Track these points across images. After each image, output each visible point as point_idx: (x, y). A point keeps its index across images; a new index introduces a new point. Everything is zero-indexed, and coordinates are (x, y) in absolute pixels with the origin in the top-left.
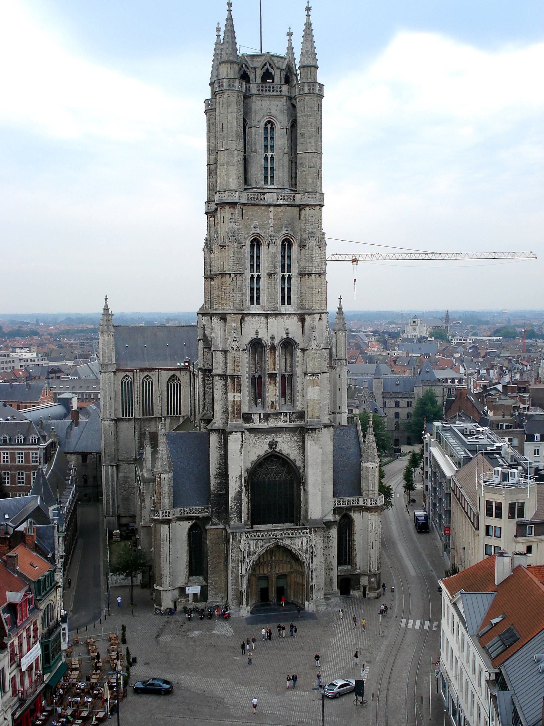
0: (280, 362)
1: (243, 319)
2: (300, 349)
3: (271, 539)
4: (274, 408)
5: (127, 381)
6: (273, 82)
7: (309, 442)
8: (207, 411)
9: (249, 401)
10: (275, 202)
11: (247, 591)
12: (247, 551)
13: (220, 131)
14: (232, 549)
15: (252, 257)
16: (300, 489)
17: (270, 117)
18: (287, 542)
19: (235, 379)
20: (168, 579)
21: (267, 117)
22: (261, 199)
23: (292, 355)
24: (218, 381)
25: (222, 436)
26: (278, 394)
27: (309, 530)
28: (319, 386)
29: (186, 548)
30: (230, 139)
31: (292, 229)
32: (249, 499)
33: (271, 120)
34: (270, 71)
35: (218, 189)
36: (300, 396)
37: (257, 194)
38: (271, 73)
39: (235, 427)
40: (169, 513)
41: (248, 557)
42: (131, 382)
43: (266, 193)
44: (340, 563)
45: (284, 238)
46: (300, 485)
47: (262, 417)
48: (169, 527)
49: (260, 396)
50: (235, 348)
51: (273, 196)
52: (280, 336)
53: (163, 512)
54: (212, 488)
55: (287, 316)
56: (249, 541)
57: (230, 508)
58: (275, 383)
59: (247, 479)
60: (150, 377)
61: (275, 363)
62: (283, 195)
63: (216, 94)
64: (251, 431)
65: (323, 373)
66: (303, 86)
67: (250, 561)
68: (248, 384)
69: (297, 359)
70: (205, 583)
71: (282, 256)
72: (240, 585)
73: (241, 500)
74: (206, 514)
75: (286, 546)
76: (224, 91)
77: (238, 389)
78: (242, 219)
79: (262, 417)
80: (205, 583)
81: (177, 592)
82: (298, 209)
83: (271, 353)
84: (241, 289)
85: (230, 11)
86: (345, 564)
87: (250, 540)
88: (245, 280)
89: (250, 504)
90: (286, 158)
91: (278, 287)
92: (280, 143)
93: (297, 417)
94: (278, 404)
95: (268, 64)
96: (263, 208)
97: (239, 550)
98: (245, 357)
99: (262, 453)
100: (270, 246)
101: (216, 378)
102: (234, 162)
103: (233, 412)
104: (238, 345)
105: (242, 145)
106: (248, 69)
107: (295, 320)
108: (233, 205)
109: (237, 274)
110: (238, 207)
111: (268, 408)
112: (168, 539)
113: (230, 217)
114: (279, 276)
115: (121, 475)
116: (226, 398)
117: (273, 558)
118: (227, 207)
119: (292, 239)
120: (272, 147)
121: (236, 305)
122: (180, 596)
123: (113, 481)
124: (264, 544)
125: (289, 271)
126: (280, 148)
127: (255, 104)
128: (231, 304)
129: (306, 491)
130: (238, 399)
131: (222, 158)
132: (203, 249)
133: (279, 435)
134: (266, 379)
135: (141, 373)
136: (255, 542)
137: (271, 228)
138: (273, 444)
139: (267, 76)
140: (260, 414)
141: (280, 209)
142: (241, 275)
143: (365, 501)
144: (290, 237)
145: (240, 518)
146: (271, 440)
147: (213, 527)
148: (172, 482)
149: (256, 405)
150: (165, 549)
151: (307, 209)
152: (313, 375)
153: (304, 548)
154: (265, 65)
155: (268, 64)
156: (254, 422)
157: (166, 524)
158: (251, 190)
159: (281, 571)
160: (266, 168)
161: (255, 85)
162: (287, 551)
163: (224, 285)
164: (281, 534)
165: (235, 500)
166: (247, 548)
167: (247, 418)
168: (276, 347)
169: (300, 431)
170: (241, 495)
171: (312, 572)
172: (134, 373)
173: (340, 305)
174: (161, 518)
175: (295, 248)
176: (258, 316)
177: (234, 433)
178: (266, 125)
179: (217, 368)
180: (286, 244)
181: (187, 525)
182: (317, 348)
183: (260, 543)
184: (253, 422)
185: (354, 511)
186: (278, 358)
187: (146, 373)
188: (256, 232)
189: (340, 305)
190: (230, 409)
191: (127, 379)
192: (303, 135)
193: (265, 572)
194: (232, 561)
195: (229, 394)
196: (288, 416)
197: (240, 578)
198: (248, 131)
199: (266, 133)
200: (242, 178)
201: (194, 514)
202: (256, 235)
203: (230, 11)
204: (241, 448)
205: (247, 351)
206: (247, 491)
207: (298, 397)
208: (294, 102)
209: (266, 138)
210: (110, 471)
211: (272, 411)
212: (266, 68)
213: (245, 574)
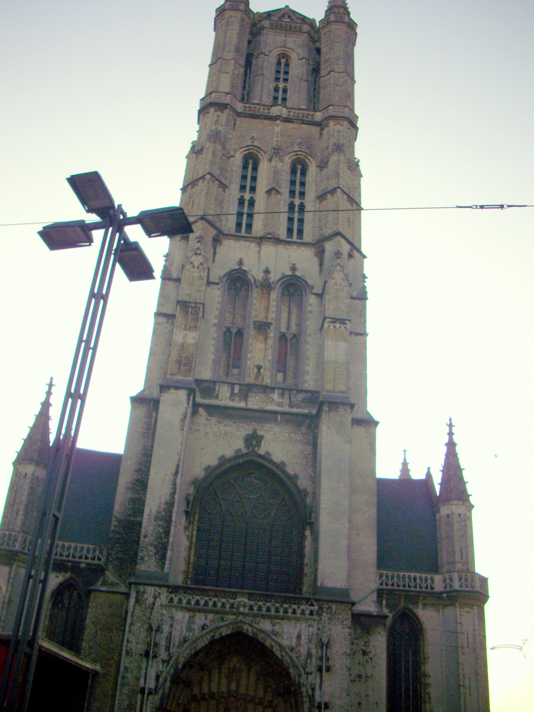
2: (315, 294)
3: (226, 613)
4: (260, 379)
9: (216, 362)
14: (132, 624)
21: (281, 49)
23: (300, 306)
26: (270, 358)
27: (316, 607)
28: (346, 341)
32: (191, 542)
37: (258, 107)
39: (179, 382)
40: (16, 540)
41: (168, 648)
45: (295, 157)
46: (304, 529)
47: (236, 390)
48: (10, 573)
50: (196, 264)
55: (295, 247)
56: (174, 610)
57: (142, 534)
58: (265, 339)
59: (191, 499)
61: (267, 309)
64: (211, 410)
67: (170, 657)
68: (215, 335)
69: (309, 308)
73: (168, 520)
74: (96, 562)
75: (261, 636)
77: (193, 325)
78: (234, 129)
79: (236, 390)
83: (262, 293)
87: (176, 607)
89: (192, 552)
90: (304, 85)
92: (296, 72)
93: (304, 401)
94: (268, 374)
96: (266, 122)
97: (146, 626)
99: (229, 453)
100: (273, 160)
103: (179, 362)
109: (217, 180)
110: (226, 111)
111: (249, 376)
117: (233, 687)
119: (308, 159)
124: (207, 622)
126: (297, 76)
127: (265, 36)
133: (267, 426)
134: (251, 333)
136: (187, 615)
140: (232, 385)
141: (291, 125)
142: (224, 187)
143: (448, 581)
144: (305, 156)
145: (162, 558)
146: (251, 432)
147: (104, 588)
151: (331, 123)
152: (335, 320)
153: (303, 650)
156: (220, 398)
165: (156, 518)
168: (273, 286)
170: (171, 512)
175: (312, 170)
176: (245, 241)
178: (279, 60)
180: (299, 167)
183: (200, 619)
184: (217, 397)
185: (424, 605)
186: (274, 303)
194: (127, 653)
196: (286, 395)
197: (139, 696)
198: (254, 62)
201: (70, 558)
202: (252, 149)
204: (183, 420)
205: (219, 286)
206: (189, 523)
208: (317, 44)
211: (258, 383)
213: (152, 686)
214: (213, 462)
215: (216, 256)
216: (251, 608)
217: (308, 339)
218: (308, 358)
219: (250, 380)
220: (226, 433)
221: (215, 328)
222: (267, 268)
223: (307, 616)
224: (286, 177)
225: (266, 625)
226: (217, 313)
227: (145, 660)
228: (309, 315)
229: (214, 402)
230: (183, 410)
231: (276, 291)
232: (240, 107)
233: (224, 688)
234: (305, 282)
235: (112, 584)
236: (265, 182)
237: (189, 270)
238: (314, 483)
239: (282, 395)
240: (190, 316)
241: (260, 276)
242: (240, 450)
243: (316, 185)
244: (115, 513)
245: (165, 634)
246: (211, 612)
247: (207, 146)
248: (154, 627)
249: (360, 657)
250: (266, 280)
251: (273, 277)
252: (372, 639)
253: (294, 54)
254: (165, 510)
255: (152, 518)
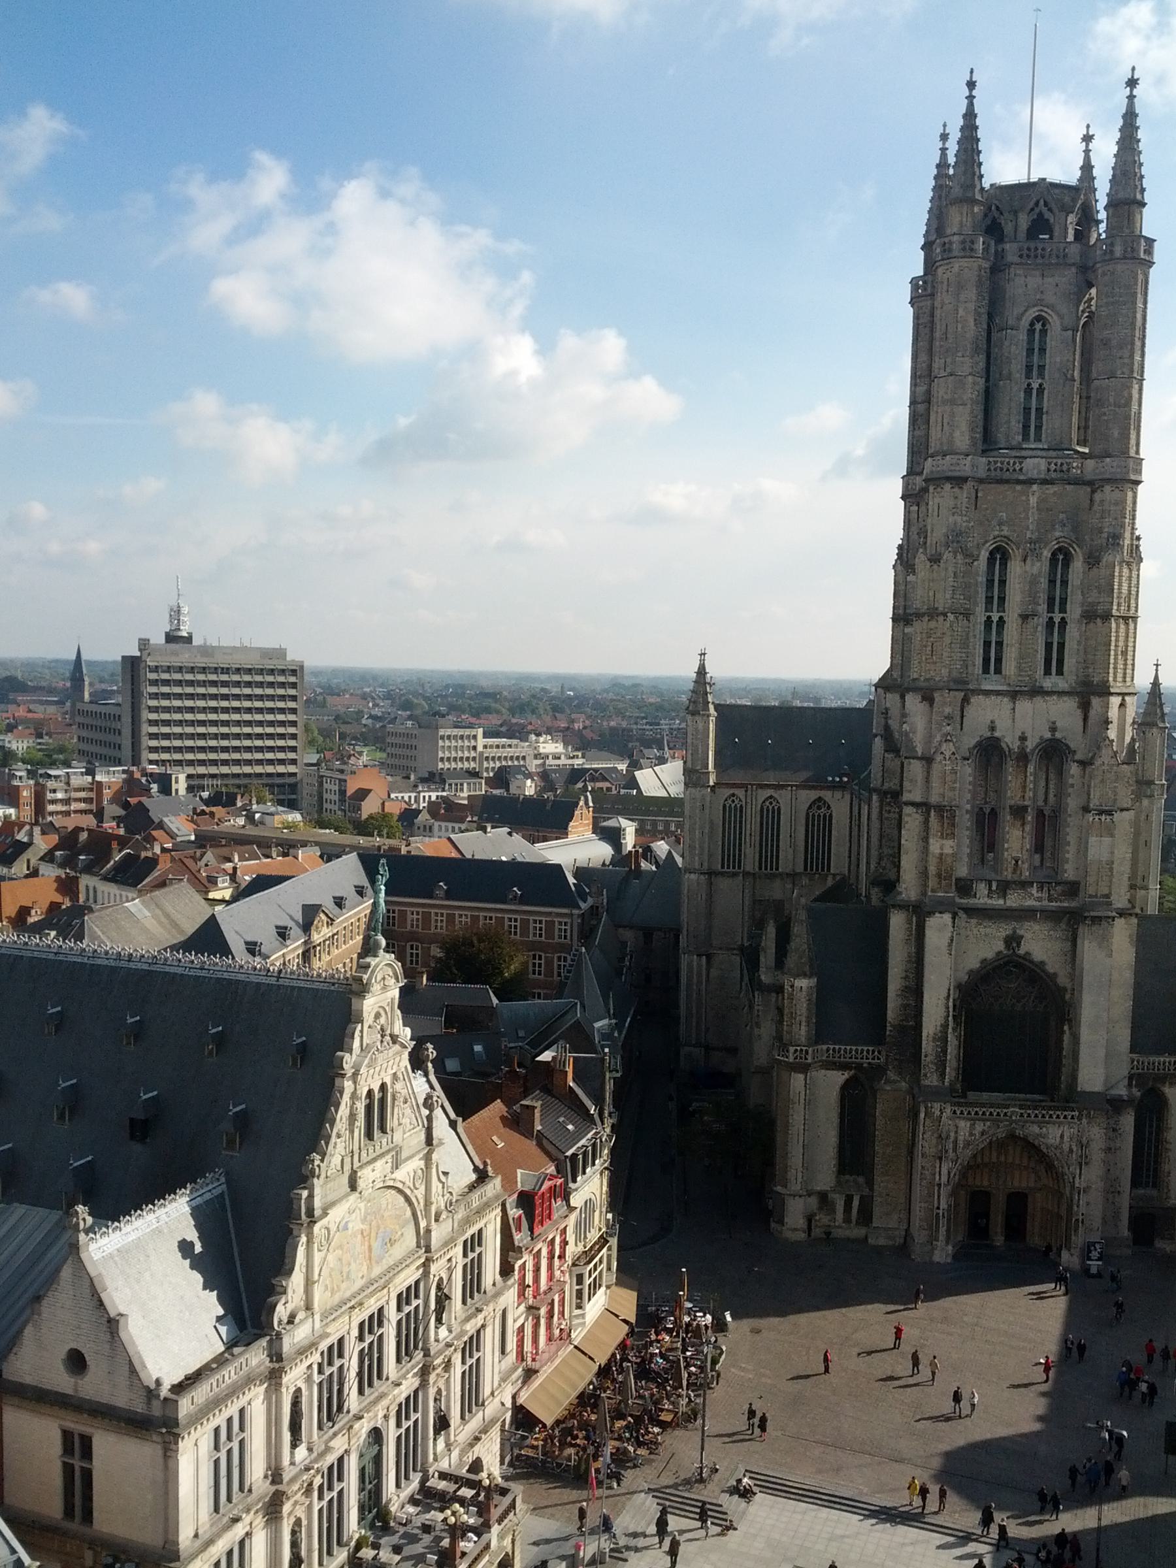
0: (1035, 784)
1: (966, 701)
4: (1018, 872)
5: (733, 805)
6: (1051, 238)
7: (1086, 942)
8: (884, 868)
9: (970, 855)
10: (1042, 476)
11: (949, 1216)
12: (951, 1140)
13: (941, 339)
14: (924, 1133)
15: (990, 583)
16: (1063, 1032)
17: (1042, 308)
18: (1035, 1129)
19: (946, 812)
20: (800, 1175)
22: (1014, 470)
23: (1060, 773)
24: (909, 815)
25: (914, 919)
26: (1028, 847)
28: (1112, 836)
29: (835, 1120)
30: (960, 354)
31: (1075, 529)
33: (1043, 314)
34: (1046, 217)
35: (931, 451)
36: (1071, 852)
37: (1007, 460)
38: (1048, 220)
41: (955, 1150)
42: (741, 806)
43: (1026, 458)
44: (1135, 1184)
45: (1056, 547)
47: (994, 888)
49: (992, 847)
51: (1039, 463)
52: (1036, 733)
53: (796, 1050)
54: (891, 1015)
55: (1055, 697)
57: (923, 1054)
58: (1023, 825)
59: (958, 1003)
60: (775, 799)
61: (1024, 787)
62: (1059, 461)
63: (937, 268)
64: (971, 912)
65: (1122, 810)
66: (1112, 244)
69: (1071, 781)
70: (866, 1192)
71: (1050, 581)
72: (936, 1202)
73: (945, 1040)
75: (1031, 1139)
76: (951, 260)
78: (976, 509)
79: (994, 888)
80: (866, 1192)
81: (813, 1201)
82: (1089, 489)
84: (965, 644)
85: (971, 98)
86: (1147, 1185)
88: (974, 625)
89: (962, 1051)
91: (1040, 641)
92: (1058, 360)
93: (1064, 893)
94: (1026, 866)
95: (1042, 202)
96: (1018, 488)
97: (936, 1135)
98: (967, 771)
99: (990, 955)
101: (908, 810)
102: (965, 398)
103: (939, 875)
104: (954, 750)
105: (982, 365)
106: (1002, 214)
107: (1069, 705)
108: (959, 481)
112: (802, 1101)
113: (952, 503)
114: (1043, 620)
115: (714, 973)
116: (925, 850)
117: (1002, 1159)
118: (948, 486)
120: (1042, 368)
121: (955, 674)
122: (820, 1209)
123: (699, 982)
124: (986, 1128)
125: (1063, 610)
128: (945, 672)
129: (1076, 1039)
130: (948, 850)
131: (941, 390)
132: (894, 567)
133: (1027, 924)
135: (760, 791)
137: (1031, 527)
138: (1013, 941)
139: (1040, 226)
141: (1052, 489)
142: (967, 615)
144: (1069, 544)
145: (942, 1075)
148: (814, 996)
149: (983, 864)
150: (797, 1117)
151: (1107, 488)
152: (1101, 813)
153: (1066, 1147)
154: (1037, 204)
155: (1042, 202)
156: (978, 896)
157: (800, 1072)
158: (995, 453)
159: (1016, 1184)
160: (1027, 410)
161: (1015, 245)
162: (1031, 1148)
163: (934, 636)
164: (1022, 1115)
165: (934, 1039)
166: (952, 1134)
167: (964, 887)
168: (1030, 757)
169: (1069, 920)
170: (946, 1033)
171: (1079, 1194)
172: (746, 791)
173: (1156, 677)
174: (791, 1059)
175: (1078, 565)
177: (937, 915)
178: (1032, 324)
179: (910, 792)
180: (1061, 557)
181: (839, 1078)
182: (1113, 761)
183: (979, 1127)
186: (1032, 778)
187: (770, 792)
188: (1002, 533)
189: (1156, 677)
190: (932, 870)
191: (733, 801)
192: (1106, 343)
193: (986, 1183)
195: (931, 841)
197: (936, 1188)
198: (995, 336)
199: (1031, 341)
200: (980, 429)
203: (971, 98)
204: (950, 945)
207: (1070, 853)
208: (1091, 277)
209: (1030, 351)
210: (695, 963)
211: (1016, 878)
212: (1037, 210)
214: (974, 964)
215: (965, 718)
216: (1022, 1115)
217: (1069, 819)
218: (1068, 844)
219: (1008, 875)
220: (986, 935)
221: (968, 816)
222: (1023, 733)
223: (1069, 1120)
224: (1044, 583)
225: (1035, 1129)
226: (969, 796)
227: (938, 1161)
228: (1070, 790)
229: (972, 901)
230: (950, 935)
231: (1033, 762)
232: (979, 465)
233: (994, 1160)
234: (1066, 745)
235: (895, 1082)
236: (1018, 598)
237: (940, 762)
238: (1072, 980)
239: (1041, 889)
240: (946, 821)
241: (1015, 745)
242: (1000, 952)
243: (1083, 594)
244: (889, 1019)
245: (952, 1139)
246: (988, 1120)
247: (945, 557)
248: (944, 1136)
249: (1111, 1134)
250: (1022, 749)
251: (1030, 745)
252: (1121, 1118)
253: (1055, 317)
254: (941, 1032)
255: (931, 1039)
